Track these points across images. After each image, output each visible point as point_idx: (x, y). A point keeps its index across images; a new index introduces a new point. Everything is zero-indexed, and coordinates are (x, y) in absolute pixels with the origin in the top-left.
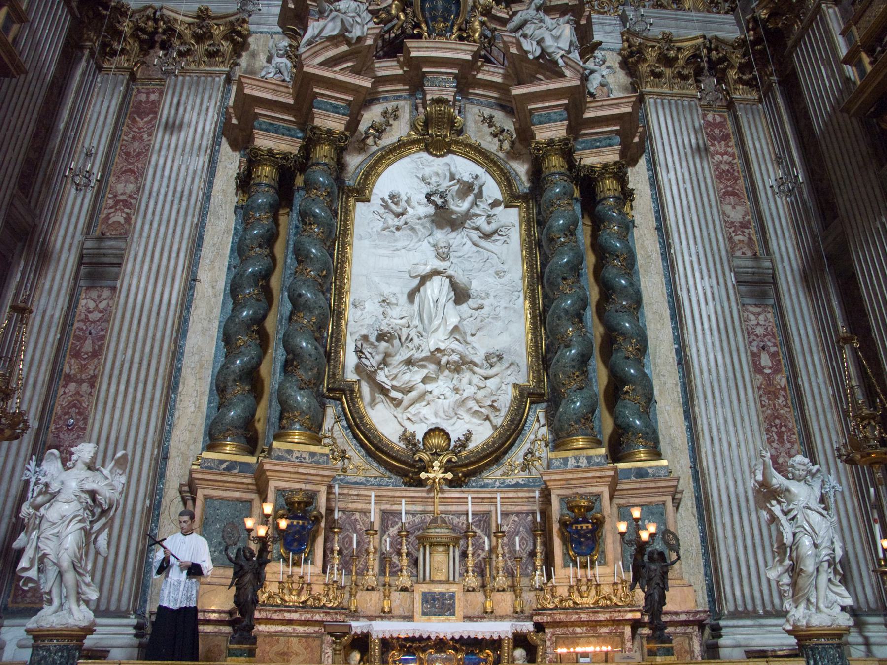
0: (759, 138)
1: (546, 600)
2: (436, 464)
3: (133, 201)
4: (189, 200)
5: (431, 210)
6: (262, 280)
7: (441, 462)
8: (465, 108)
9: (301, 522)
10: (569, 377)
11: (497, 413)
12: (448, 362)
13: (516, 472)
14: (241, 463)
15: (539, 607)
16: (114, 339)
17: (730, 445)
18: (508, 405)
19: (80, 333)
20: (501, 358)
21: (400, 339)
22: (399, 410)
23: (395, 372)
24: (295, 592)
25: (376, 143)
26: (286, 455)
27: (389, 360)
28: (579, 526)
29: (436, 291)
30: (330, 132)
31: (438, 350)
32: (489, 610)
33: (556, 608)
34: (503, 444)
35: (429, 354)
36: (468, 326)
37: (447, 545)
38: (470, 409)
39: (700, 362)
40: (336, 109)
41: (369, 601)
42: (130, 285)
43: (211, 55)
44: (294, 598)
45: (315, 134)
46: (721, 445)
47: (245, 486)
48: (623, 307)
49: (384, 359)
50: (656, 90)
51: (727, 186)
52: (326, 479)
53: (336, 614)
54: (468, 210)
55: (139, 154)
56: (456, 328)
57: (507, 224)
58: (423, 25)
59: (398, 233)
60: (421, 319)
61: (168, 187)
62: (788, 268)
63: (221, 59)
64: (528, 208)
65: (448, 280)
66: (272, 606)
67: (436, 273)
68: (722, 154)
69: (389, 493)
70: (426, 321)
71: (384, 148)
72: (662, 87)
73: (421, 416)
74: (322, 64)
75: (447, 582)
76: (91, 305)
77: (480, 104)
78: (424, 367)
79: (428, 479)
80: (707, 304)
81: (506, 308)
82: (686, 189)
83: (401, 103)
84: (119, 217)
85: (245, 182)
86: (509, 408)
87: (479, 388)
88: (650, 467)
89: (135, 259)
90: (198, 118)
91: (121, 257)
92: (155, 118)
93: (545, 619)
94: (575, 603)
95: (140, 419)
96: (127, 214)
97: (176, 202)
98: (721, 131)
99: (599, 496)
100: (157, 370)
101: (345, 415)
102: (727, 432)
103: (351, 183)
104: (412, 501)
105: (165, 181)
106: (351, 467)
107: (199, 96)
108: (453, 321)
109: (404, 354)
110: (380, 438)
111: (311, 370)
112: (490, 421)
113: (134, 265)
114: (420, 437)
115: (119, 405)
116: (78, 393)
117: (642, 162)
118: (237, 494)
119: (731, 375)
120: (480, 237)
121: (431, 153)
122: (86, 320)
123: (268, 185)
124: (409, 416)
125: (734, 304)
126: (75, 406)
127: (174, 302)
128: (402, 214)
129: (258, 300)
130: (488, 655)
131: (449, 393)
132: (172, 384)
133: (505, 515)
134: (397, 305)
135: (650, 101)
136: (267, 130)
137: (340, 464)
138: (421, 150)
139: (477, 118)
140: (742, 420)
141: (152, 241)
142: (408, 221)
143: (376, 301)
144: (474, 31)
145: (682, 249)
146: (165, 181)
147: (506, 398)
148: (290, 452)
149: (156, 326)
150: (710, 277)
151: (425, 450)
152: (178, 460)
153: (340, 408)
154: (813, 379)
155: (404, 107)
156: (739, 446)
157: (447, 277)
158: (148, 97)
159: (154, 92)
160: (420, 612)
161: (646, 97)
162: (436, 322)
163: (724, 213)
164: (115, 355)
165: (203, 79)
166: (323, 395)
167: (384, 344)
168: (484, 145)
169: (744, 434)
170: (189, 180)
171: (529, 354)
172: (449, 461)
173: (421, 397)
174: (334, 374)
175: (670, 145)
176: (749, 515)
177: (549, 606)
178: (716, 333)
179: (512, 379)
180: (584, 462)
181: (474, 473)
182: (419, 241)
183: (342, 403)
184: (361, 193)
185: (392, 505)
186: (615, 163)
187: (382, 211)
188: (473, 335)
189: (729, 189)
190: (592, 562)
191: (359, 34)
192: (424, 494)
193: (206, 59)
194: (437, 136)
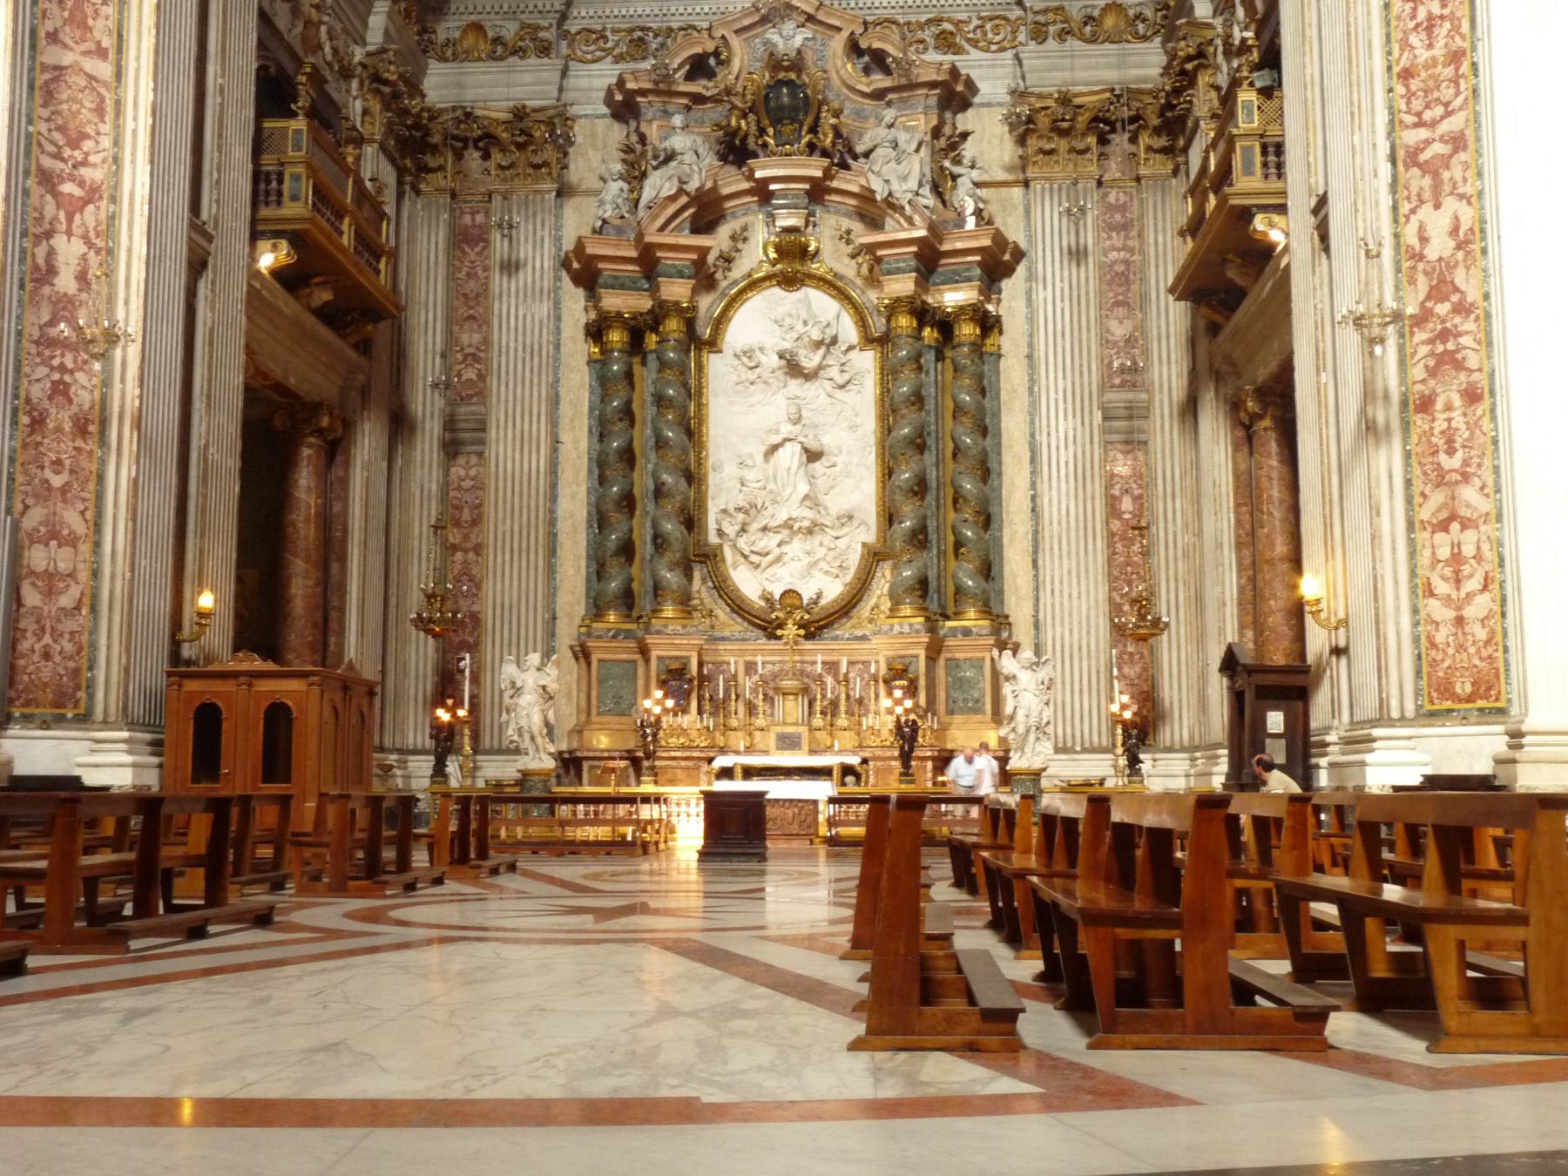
0: (1164, 230)
2: (790, 622)
3: (482, 355)
4: (540, 357)
5: (783, 362)
14: (627, 631)
17: (1070, 596)
18: (857, 563)
19: (456, 502)
22: (759, 570)
23: (753, 538)
30: (677, 303)
31: (790, 519)
39: (1051, 512)
40: (681, 275)
42: (497, 455)
43: (537, 167)
46: (1062, 596)
51: (1118, 294)
55: (478, 295)
56: (806, 497)
58: (771, 131)
59: (752, 388)
61: (516, 341)
62: (1166, 401)
67: (787, 440)
68: (1119, 250)
75: (796, 724)
76: (462, 472)
77: (837, 212)
80: (1066, 448)
82: (1062, 310)
84: (470, 374)
85: (595, 332)
87: (830, 549)
89: (498, 427)
90: (534, 252)
91: (484, 422)
92: (485, 248)
95: (528, 587)
96: (479, 370)
97: (528, 358)
98: (1123, 216)
99: (917, 656)
100: (537, 539)
102: (1070, 583)
105: (512, 332)
107: (531, 220)
108: (803, 488)
110: (743, 599)
113: (497, 433)
114: (777, 596)
115: (507, 574)
116: (465, 561)
117: (1021, 270)
118: (624, 656)
119: (1081, 525)
122: (459, 488)
125: (1096, 447)
126: (465, 574)
127: (542, 469)
128: (756, 367)
131: (802, 556)
132: (552, 552)
133: (851, 663)
135: (1036, 186)
137: (708, 621)
139: (835, 233)
140: (1087, 571)
141: (511, 403)
144: (826, 136)
145: (1048, 386)
146: (512, 332)
147: (854, 559)
149: (529, 495)
150: (1074, 417)
152: (566, 620)
153: (705, 570)
154: (1170, 525)
156: (1079, 598)
158: (473, 220)
159: (478, 212)
161: (1032, 184)
162: (788, 492)
163: (1108, 331)
164: (496, 527)
165: (531, 197)
166: (690, 560)
167: (741, 516)
169: (1088, 585)
170: (537, 330)
171: (878, 513)
173: (778, 560)
175: (1053, 251)
176: (1081, 662)
178: (1072, 480)
180: (906, 629)
181: (825, 626)
184: (713, 344)
187: (736, 362)
189: (1121, 298)
193: (531, 171)
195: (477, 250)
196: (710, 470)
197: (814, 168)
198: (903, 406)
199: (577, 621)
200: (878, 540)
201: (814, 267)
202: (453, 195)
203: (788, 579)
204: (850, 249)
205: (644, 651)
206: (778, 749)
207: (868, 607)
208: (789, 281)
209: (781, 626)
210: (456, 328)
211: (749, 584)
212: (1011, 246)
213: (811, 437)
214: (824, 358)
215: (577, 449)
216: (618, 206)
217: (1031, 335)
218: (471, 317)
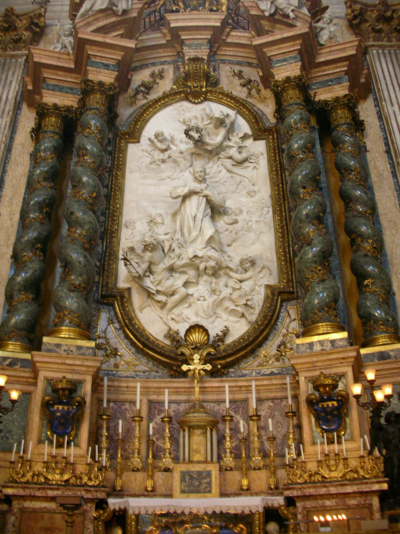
1: (295, 475)
2: (196, 357)
5: (191, 145)
6: (46, 207)
7: (201, 355)
8: (219, 67)
9: (66, 408)
10: (312, 271)
11: (252, 311)
12: (206, 268)
13: (270, 362)
15: (290, 482)
18: (261, 304)
20: (254, 264)
21: (163, 251)
22: (165, 311)
23: (159, 278)
24: (58, 471)
25: (145, 98)
26: (55, 348)
27: (154, 268)
28: (325, 404)
29: (194, 209)
30: (101, 84)
31: (196, 256)
32: (245, 488)
33: (306, 482)
34: (257, 337)
35: (188, 261)
36: (225, 238)
37: (203, 428)
38: (227, 308)
40: (106, 66)
44: (57, 477)
45: (88, 85)
47: (25, 380)
48: (360, 213)
49: (149, 267)
50: (377, 43)
52: (91, 369)
53: (96, 491)
54: (222, 143)
56: (211, 238)
57: (256, 153)
59: (163, 166)
60: (182, 234)
63: (23, 45)
64: (273, 139)
65: (204, 200)
66: (36, 484)
67: (192, 193)
69: (156, 385)
70: (186, 235)
71: (151, 101)
72: (382, 41)
73: (184, 316)
74: (94, 31)
75: (206, 462)
77: (231, 63)
78: (184, 273)
79: (189, 370)
81: (257, 222)
83: (166, 67)
86: (263, 306)
87: (234, 289)
88: (392, 351)
93: (295, 493)
94: (323, 477)
101: (117, 318)
103: (124, 129)
104: (177, 391)
106: (123, 363)
108: (209, 231)
109: (167, 262)
111: (81, 275)
112: (246, 319)
114: (182, 334)
120: (233, 165)
121: (191, 102)
123: (53, 132)
124: (173, 316)
128: (166, 150)
129: (42, 223)
130: (242, 529)
133: (260, 401)
134: (163, 223)
138: (182, 100)
142: (171, 155)
143: (145, 222)
148: (58, 346)
151: (187, 346)
153: (112, 313)
155: (168, 70)
157: (204, 196)
160: (178, 490)
162: (194, 234)
167: (148, 255)
168: (235, 93)
172: (209, 354)
174: (107, 283)
175: (393, 85)
177: (298, 481)
179: (265, 281)
182: (182, 171)
183: (114, 309)
185: (159, 395)
186: (345, 96)
188: (229, 246)
190: (339, 437)
191: (124, 7)
192: (187, 385)
194: (194, 87)
196: (123, 227)
198: (300, 152)
200: (280, 281)
204: (242, 81)
206: (183, 492)
207: (275, 347)
215: (11, 219)
216: (65, 47)
217: (386, 139)
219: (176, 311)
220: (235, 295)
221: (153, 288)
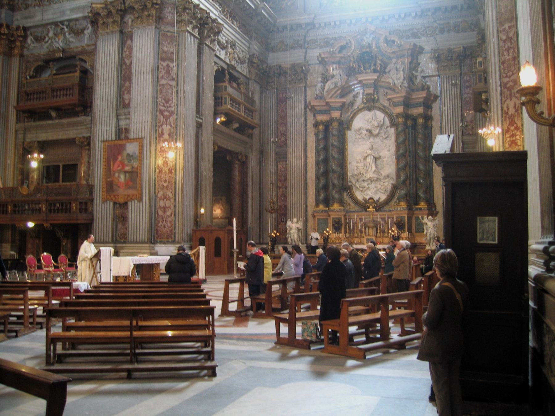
2: (371, 207)
16: (289, 177)
29: (369, 160)
30: (336, 118)
41: (356, 240)
56: (375, 171)
59: (360, 140)
67: (368, 155)
75: (372, 236)
85: (316, 125)
87: (382, 186)
109: (362, 179)
114: (367, 199)
116: (283, 191)
133: (388, 218)
136: (319, 114)
147: (389, 187)
167: (356, 177)
184: (349, 128)
195: (284, 104)
197: (375, 76)
199: (313, 207)
201: (377, 105)
202: (277, 89)
203: (371, 195)
205: (329, 216)
208: (370, 109)
209: (369, 208)
210: (279, 127)
211: (359, 196)
212: (433, 95)
213: (376, 153)
214: (380, 130)
217: (441, 121)
218: (283, 123)
219: (365, 192)
220: (382, 188)
221: (358, 187)
